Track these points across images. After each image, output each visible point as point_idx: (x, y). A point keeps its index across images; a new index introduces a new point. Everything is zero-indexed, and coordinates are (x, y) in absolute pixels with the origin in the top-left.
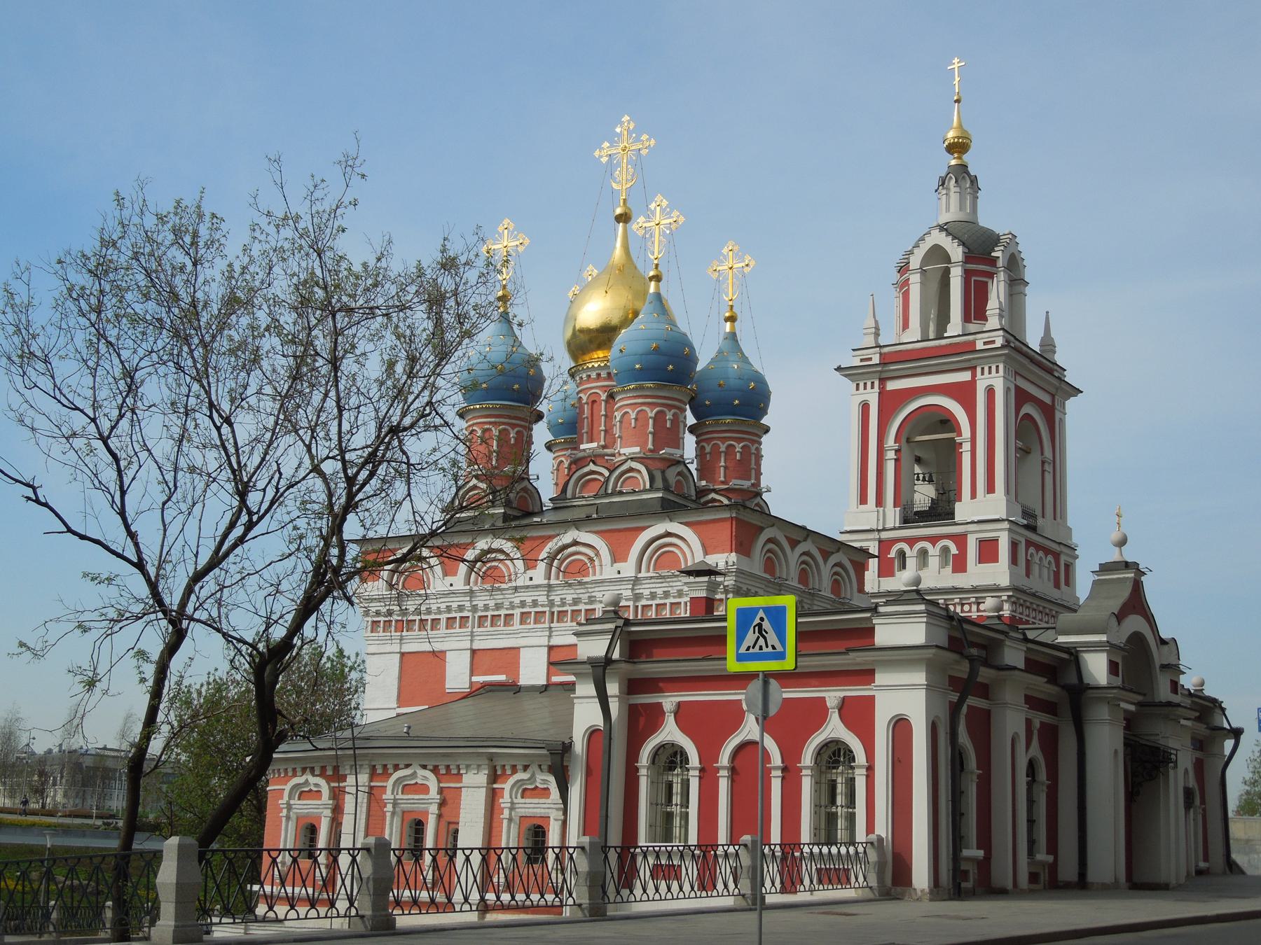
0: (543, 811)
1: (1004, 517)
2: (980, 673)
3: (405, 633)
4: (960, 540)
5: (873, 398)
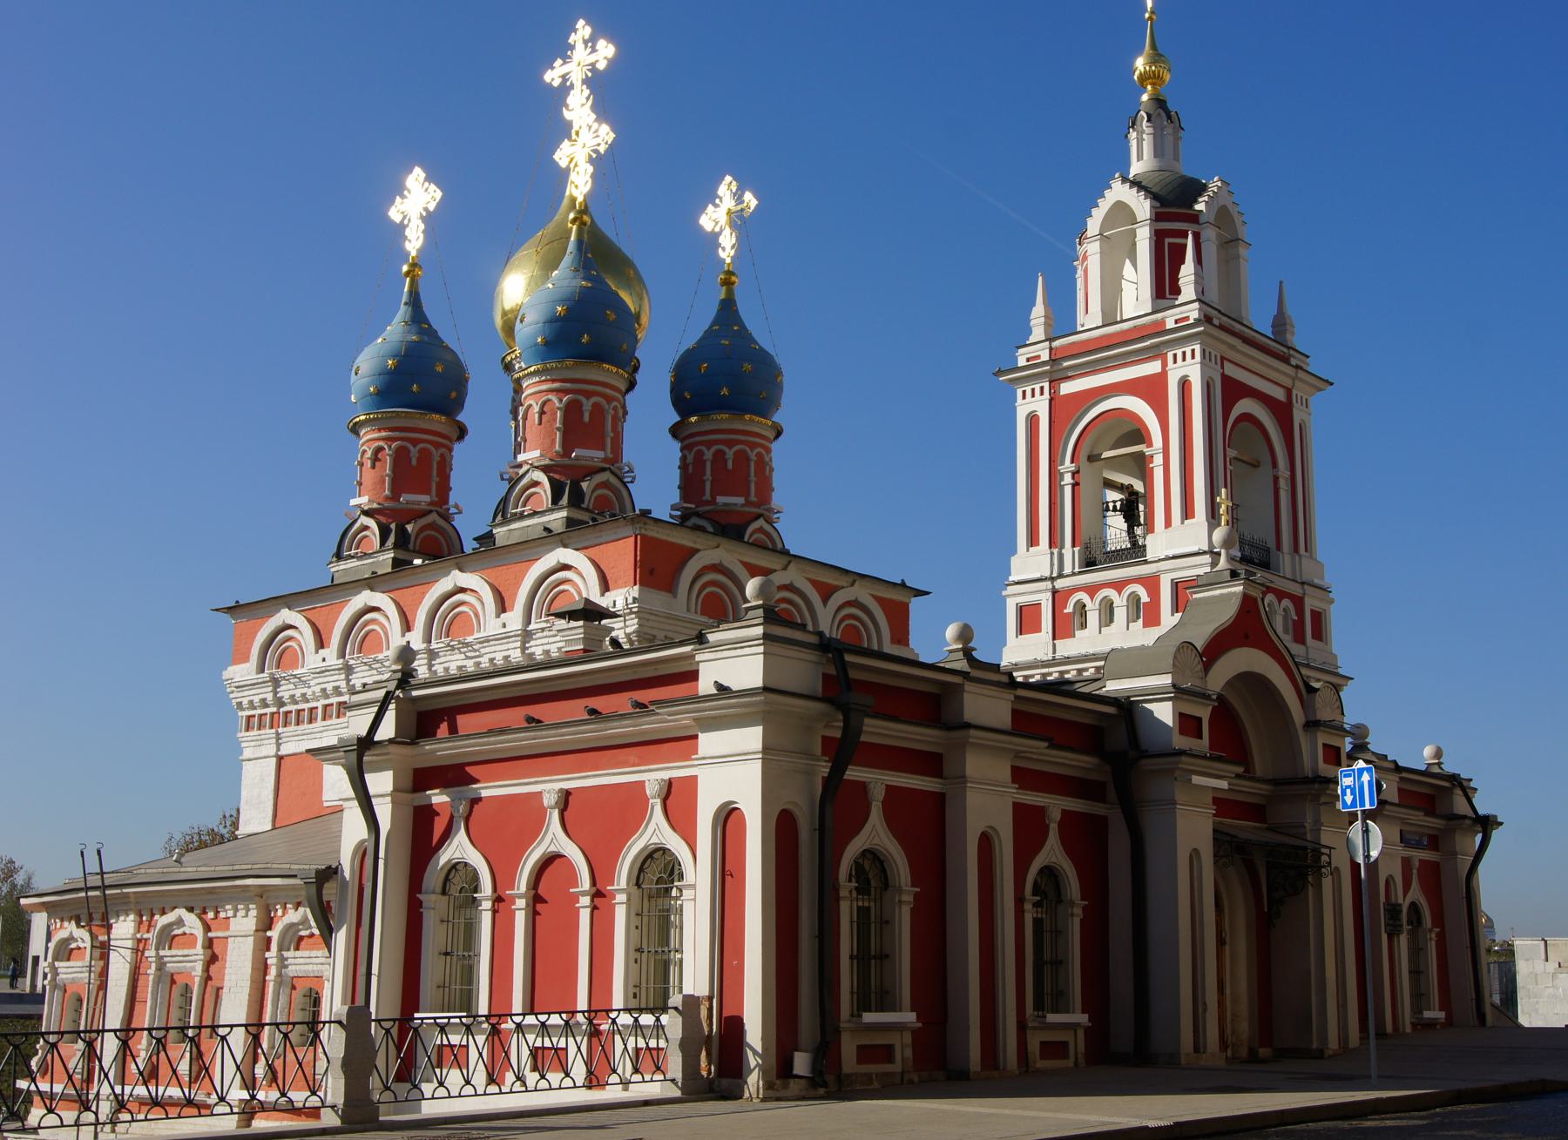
0: (315, 967)
2: (865, 728)
3: (280, 730)
4: (1151, 583)
5: (1041, 406)
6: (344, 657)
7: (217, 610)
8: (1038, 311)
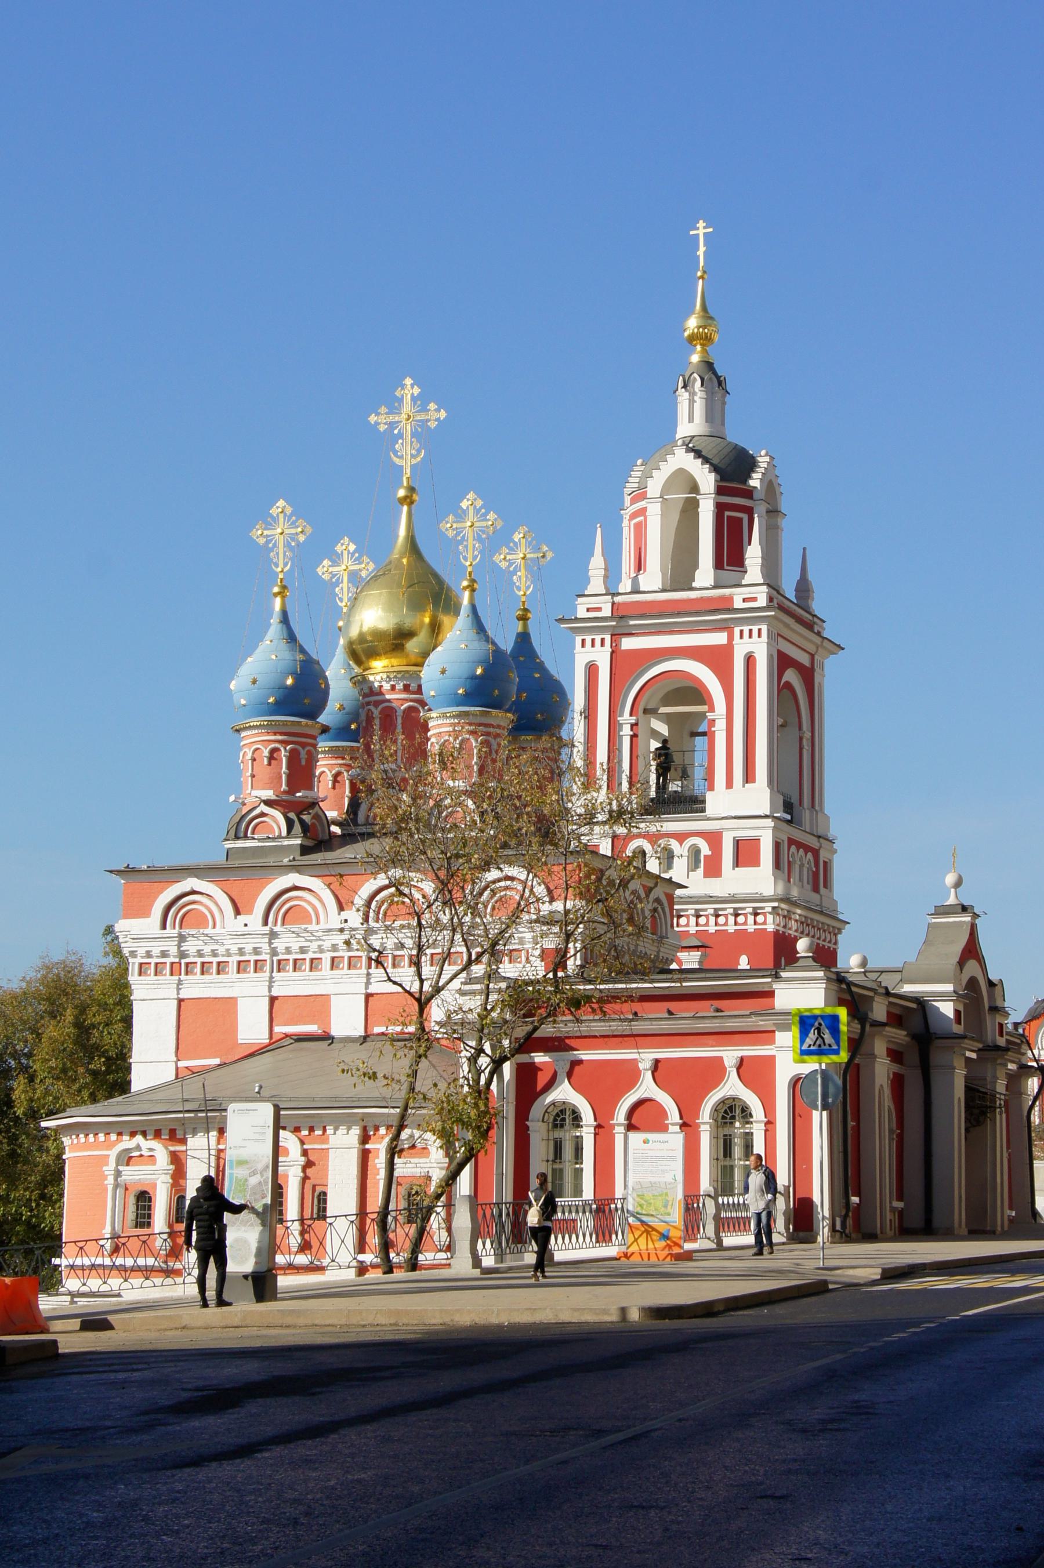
1: (768, 813)
3: (183, 977)
4: (714, 839)
6: (266, 923)
7: (111, 872)
8: (597, 563)
